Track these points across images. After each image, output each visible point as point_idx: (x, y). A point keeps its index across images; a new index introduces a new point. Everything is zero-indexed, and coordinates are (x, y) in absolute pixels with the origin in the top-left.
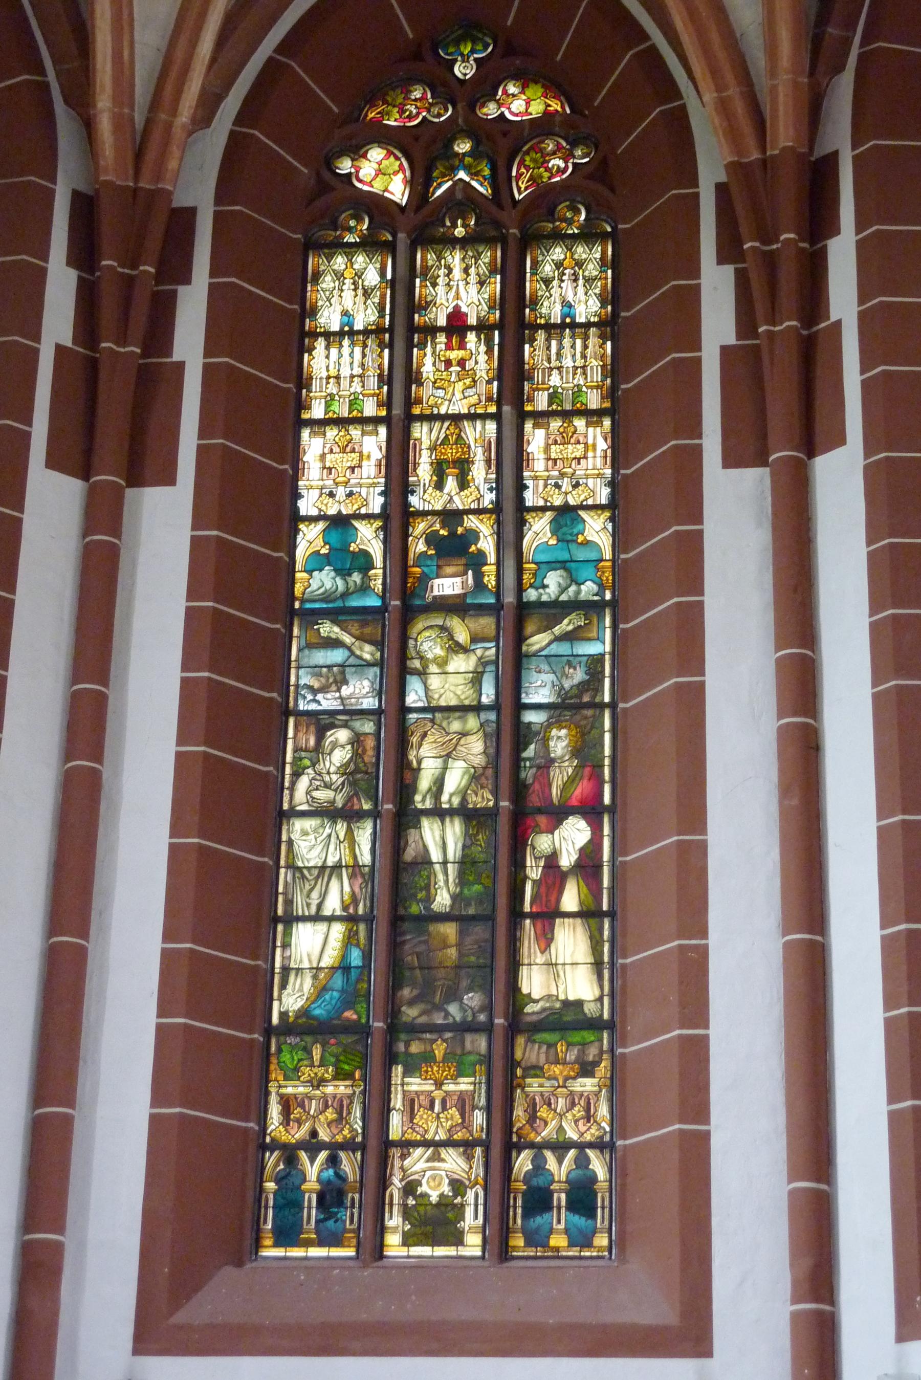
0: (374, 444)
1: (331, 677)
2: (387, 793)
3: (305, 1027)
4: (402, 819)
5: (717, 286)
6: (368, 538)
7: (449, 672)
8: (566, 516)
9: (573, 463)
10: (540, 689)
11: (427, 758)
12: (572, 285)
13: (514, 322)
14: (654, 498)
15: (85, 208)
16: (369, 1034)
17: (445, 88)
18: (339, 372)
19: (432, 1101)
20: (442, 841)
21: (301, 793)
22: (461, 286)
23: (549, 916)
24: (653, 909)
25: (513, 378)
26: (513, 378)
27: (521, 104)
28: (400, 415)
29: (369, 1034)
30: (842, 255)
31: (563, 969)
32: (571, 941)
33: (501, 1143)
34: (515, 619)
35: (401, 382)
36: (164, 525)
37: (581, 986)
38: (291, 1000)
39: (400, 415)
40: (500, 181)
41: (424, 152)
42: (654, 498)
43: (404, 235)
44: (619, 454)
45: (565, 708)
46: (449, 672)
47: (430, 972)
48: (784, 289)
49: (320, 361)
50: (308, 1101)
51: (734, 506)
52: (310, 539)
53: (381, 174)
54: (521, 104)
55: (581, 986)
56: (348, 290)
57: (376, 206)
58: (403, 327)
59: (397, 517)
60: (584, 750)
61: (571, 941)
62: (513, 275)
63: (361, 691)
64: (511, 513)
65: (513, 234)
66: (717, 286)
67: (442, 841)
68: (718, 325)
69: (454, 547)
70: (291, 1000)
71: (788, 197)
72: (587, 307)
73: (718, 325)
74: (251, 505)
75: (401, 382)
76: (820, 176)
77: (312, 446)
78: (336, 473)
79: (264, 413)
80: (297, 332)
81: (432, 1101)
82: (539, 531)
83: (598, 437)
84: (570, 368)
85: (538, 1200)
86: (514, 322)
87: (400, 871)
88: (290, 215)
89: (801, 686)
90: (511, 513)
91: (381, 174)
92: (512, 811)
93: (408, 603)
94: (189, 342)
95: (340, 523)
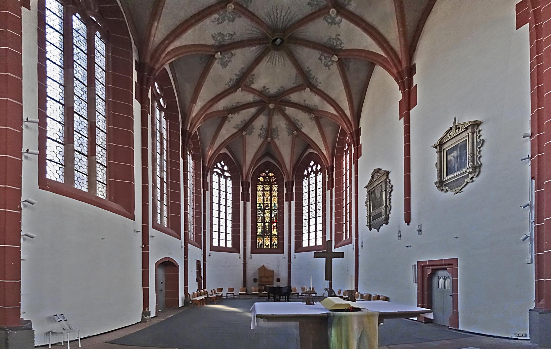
0: (262, 198)
1: (260, 214)
2: (263, 221)
3: (259, 235)
4: (264, 223)
5: (285, 189)
6: (262, 205)
7: (267, 214)
8: (275, 204)
9: (275, 200)
10: (273, 215)
11: (266, 219)
12: (275, 188)
13: (271, 190)
14: (281, 203)
15: (242, 182)
16: (263, 236)
17: (266, 173)
18: (259, 193)
19: (267, 240)
20: (267, 224)
21: (258, 221)
22: (267, 188)
23: (274, 229)
24: (281, 229)
25: (271, 194)
26: (271, 194)
27: (271, 174)
28: (263, 197)
29: (263, 236)
30: (294, 188)
31: (275, 232)
32: (275, 230)
33: (271, 242)
34: (271, 210)
35: (263, 194)
36: (249, 204)
37: (276, 233)
38: (258, 234)
39: (263, 197)
40: (270, 180)
41: (264, 178)
42: (281, 203)
43: (263, 183)
44: (278, 200)
45: (274, 216)
46: (267, 214)
47: (266, 232)
48: (290, 190)
49: (258, 193)
50: (259, 240)
51: (286, 204)
52: (258, 205)
53: (261, 179)
54: (271, 174)
55: (276, 233)
56: (259, 188)
57: (261, 182)
58: (263, 190)
59: (263, 204)
60: (276, 219)
61: (275, 230)
62: (271, 187)
63: (262, 215)
64: (271, 204)
65: (271, 184)
66: (285, 189)
67: (267, 224)
68: (285, 192)
69: (267, 206)
70: (258, 234)
71: (291, 184)
72: (276, 190)
73: (285, 192)
74: (254, 203)
75: (263, 194)
76: (293, 182)
77: (258, 198)
78: (259, 200)
79: (255, 196)
80: (256, 191)
81: (267, 240)
82: (273, 205)
83: (277, 198)
84: (275, 194)
85: (273, 245)
86: (271, 190)
87: (264, 227)
88: (256, 182)
89: (290, 216)
90: (271, 204)
91: (261, 179)
92: (271, 222)
93: (264, 209)
94: (250, 192)
95: (260, 204)
